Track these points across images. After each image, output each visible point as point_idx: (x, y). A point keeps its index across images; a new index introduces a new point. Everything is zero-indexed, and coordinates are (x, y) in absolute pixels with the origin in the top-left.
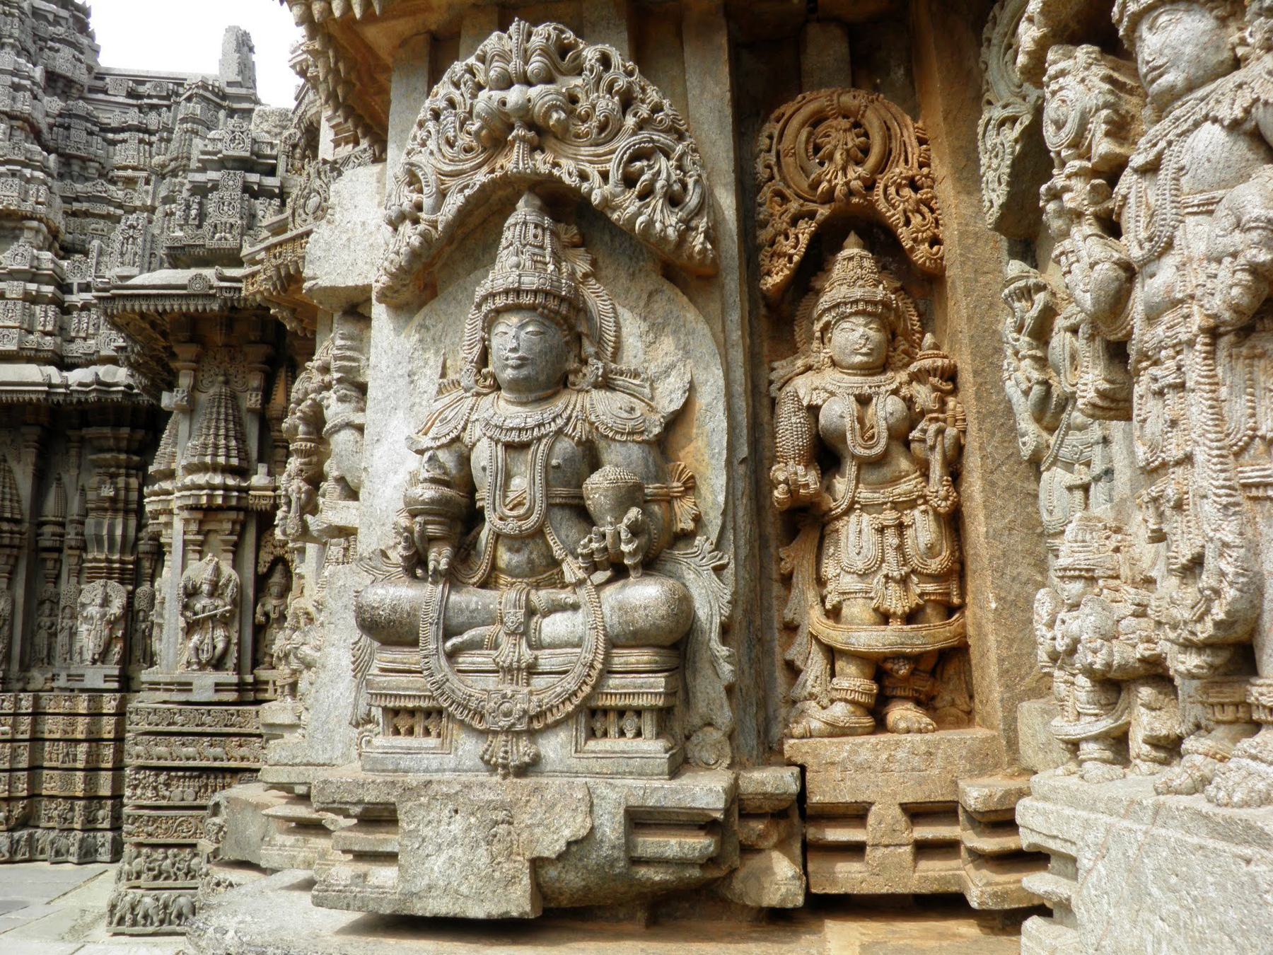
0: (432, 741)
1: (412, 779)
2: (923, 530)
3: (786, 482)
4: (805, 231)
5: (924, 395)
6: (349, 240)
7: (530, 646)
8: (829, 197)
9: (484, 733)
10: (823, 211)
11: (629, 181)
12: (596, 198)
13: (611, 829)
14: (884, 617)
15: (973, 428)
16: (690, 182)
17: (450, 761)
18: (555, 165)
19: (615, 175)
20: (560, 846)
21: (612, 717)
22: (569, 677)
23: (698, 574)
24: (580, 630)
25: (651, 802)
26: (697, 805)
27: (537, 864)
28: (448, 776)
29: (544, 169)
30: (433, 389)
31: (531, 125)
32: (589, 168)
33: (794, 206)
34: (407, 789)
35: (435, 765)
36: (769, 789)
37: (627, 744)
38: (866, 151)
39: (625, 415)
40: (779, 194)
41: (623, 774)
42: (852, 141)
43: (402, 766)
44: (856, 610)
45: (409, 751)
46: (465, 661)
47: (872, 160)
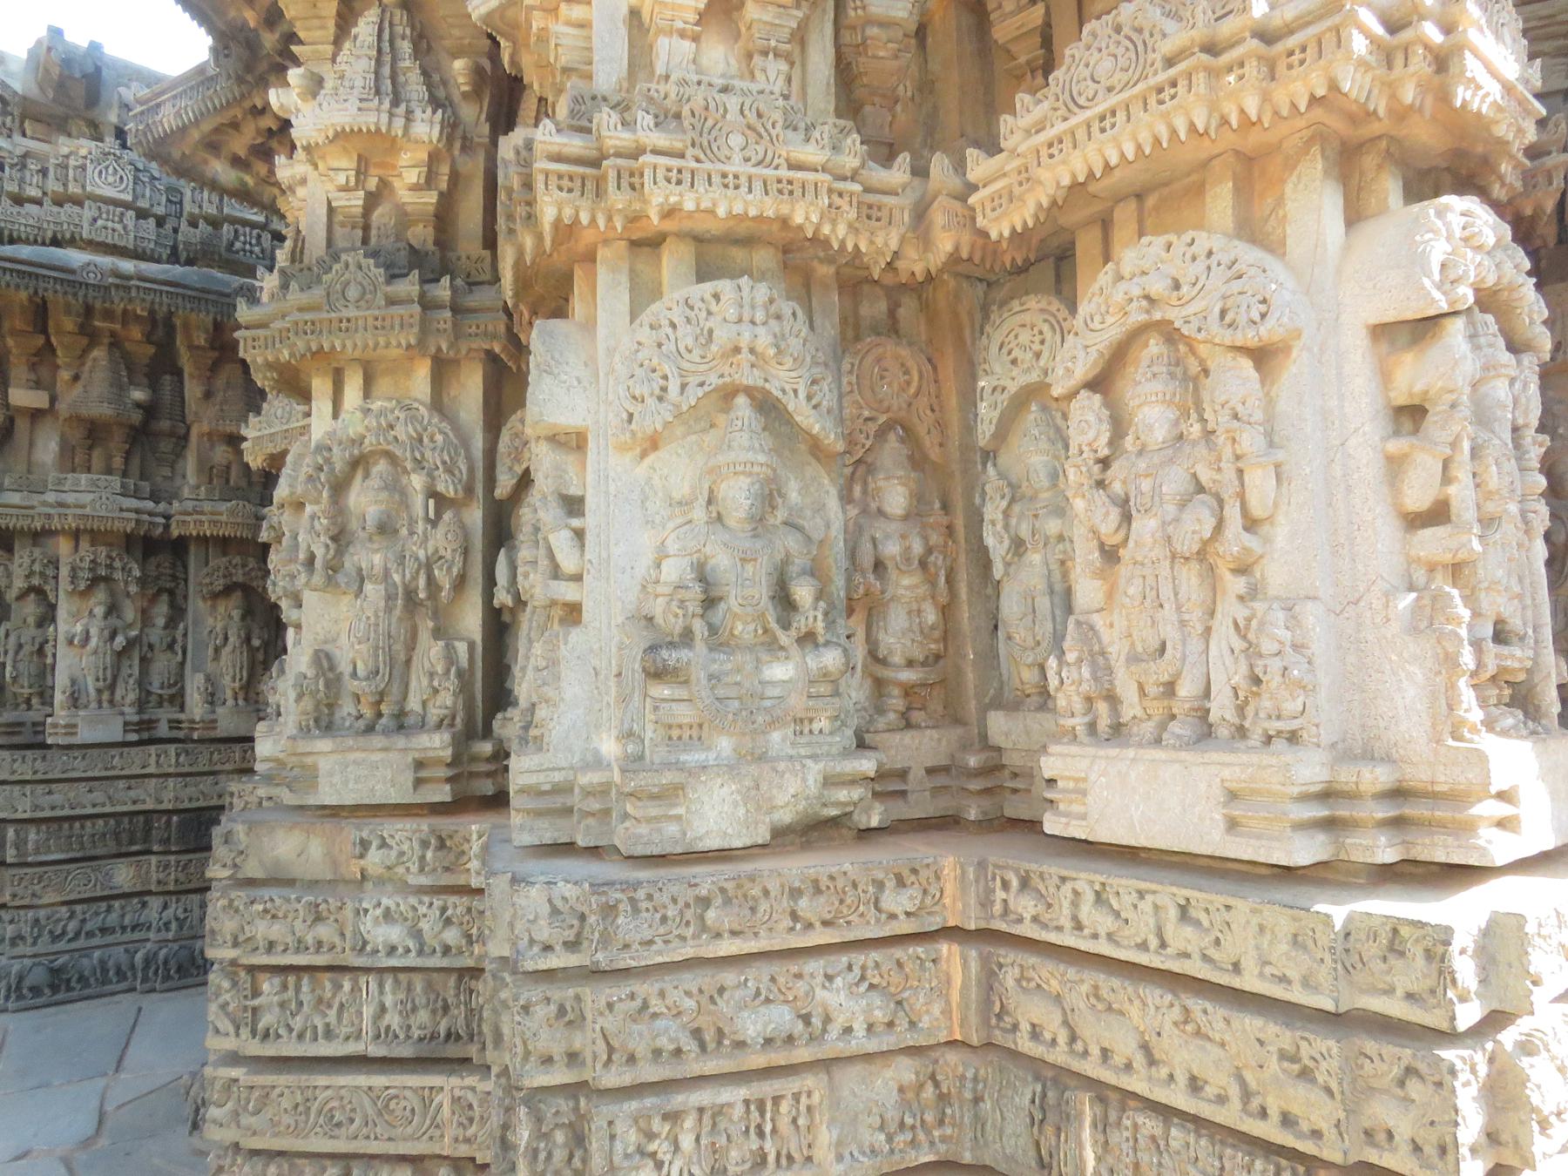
2: (931, 616)
4: (872, 428)
5: (935, 539)
8: (888, 410)
10: (883, 419)
12: (791, 408)
14: (910, 663)
15: (962, 559)
19: (802, 395)
29: (760, 383)
31: (752, 351)
32: (787, 387)
33: (866, 413)
38: (908, 383)
40: (857, 402)
42: (903, 378)
44: (897, 659)
47: (912, 390)
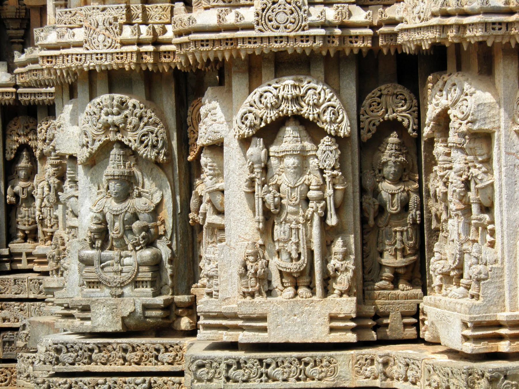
0: (99, 290)
1: (94, 299)
3: (192, 218)
6: (69, 138)
7: (121, 266)
9: (111, 287)
11: (142, 142)
13: (139, 310)
16: (159, 139)
17: (103, 294)
18: (123, 137)
19: (138, 141)
20: (128, 313)
21: (141, 283)
22: (129, 273)
23: (163, 246)
24: (132, 262)
25: (147, 303)
26: (158, 303)
27: (123, 318)
28: (103, 298)
30: (96, 194)
34: (93, 301)
35: (99, 295)
36: (182, 300)
37: (144, 289)
39: (144, 206)
41: (142, 296)
43: (91, 295)
45: (93, 292)
46: (106, 269)
